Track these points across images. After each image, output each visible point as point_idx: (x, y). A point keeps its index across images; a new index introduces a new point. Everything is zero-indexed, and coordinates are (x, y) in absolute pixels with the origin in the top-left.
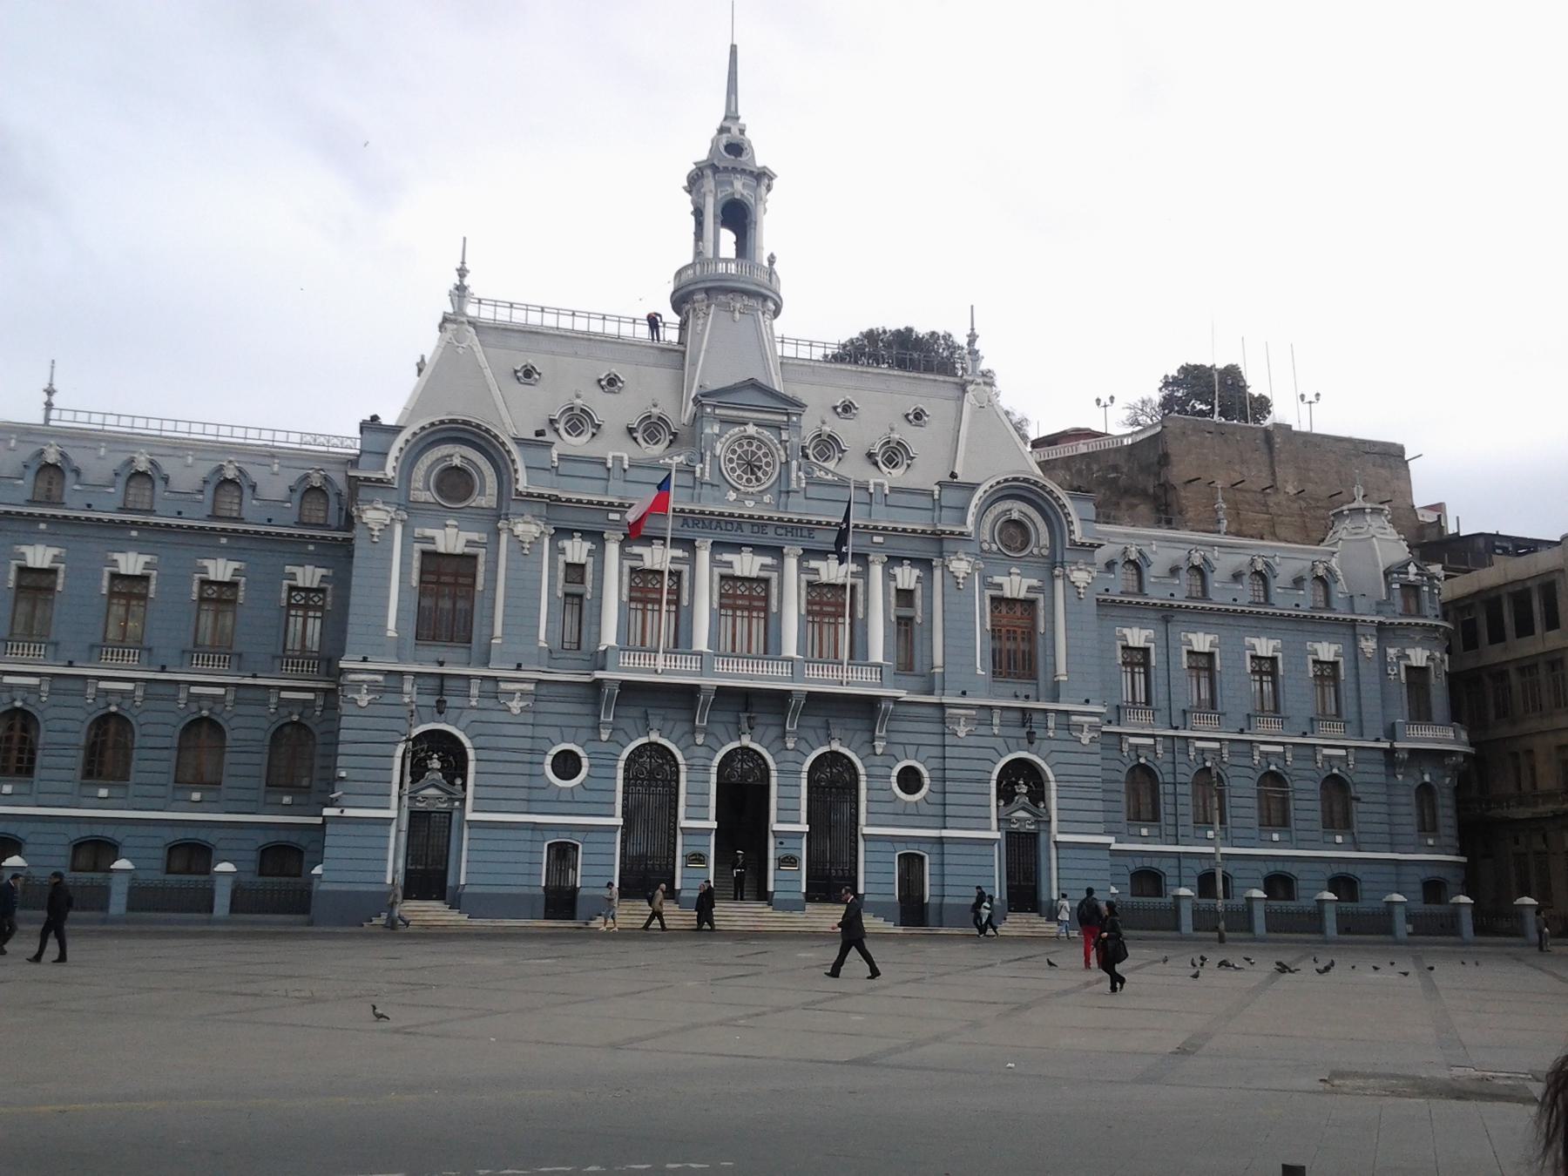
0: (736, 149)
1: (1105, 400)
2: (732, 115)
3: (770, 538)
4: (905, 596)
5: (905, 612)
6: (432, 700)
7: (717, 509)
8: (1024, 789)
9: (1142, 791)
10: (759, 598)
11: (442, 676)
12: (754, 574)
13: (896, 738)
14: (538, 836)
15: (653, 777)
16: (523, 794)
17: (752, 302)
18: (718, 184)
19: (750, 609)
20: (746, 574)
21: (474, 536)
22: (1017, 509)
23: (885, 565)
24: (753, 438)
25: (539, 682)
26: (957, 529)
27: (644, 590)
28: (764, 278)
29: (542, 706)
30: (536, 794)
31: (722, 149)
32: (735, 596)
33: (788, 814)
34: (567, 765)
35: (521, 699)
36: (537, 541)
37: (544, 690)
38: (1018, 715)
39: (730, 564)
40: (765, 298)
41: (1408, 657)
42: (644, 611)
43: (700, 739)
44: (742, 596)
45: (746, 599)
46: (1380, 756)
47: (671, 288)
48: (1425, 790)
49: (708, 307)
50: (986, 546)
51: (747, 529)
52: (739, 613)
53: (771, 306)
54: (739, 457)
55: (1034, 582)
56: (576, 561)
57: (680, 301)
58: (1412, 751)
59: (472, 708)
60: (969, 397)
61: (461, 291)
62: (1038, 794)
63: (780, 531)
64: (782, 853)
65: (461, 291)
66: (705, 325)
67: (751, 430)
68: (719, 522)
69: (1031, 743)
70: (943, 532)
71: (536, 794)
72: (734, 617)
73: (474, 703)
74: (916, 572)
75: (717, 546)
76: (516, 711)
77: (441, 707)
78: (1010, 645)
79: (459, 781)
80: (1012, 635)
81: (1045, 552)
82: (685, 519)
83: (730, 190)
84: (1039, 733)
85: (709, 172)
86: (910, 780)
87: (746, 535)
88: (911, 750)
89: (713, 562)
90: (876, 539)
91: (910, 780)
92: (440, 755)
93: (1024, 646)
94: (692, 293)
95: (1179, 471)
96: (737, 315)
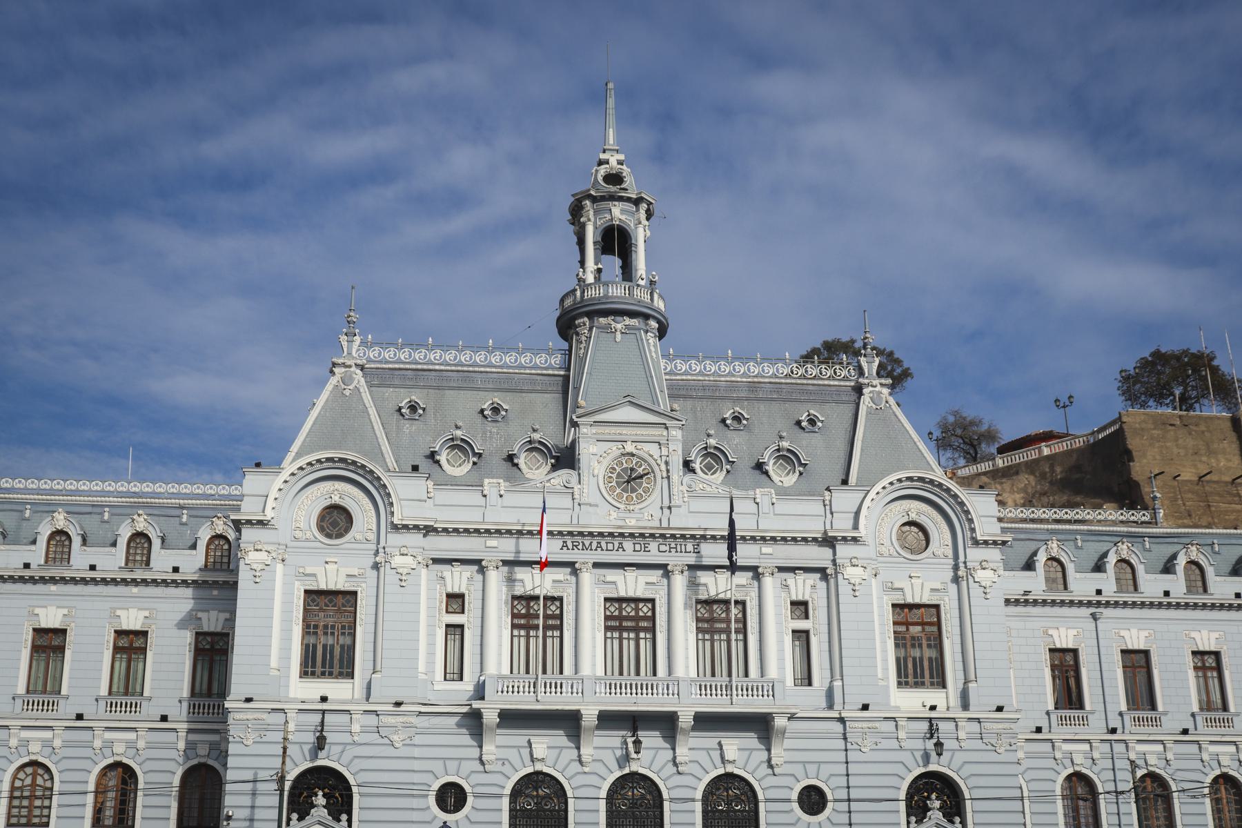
1: (1064, 400)
3: (654, 554)
4: (801, 607)
5: (802, 625)
6: (311, 738)
8: (937, 804)
10: (645, 618)
11: (324, 712)
12: (640, 594)
17: (634, 322)
18: (596, 212)
19: (637, 630)
20: (631, 594)
22: (918, 510)
24: (633, 455)
27: (528, 616)
28: (647, 298)
31: (600, 179)
32: (620, 618)
34: (452, 797)
38: (925, 726)
40: (647, 317)
42: (528, 637)
44: (628, 618)
45: (630, 620)
47: (558, 313)
49: (591, 329)
50: (884, 550)
52: (625, 635)
53: (654, 324)
54: (619, 476)
56: (456, 590)
57: (566, 326)
60: (866, 401)
62: (954, 805)
66: (587, 349)
67: (630, 448)
69: (939, 754)
70: (835, 538)
72: (621, 639)
77: (321, 743)
78: (916, 653)
79: (344, 817)
80: (915, 642)
83: (609, 217)
84: (948, 744)
86: (813, 800)
87: (629, 553)
91: (813, 800)
93: (929, 653)
94: (575, 318)
95: (1140, 469)
96: (619, 336)
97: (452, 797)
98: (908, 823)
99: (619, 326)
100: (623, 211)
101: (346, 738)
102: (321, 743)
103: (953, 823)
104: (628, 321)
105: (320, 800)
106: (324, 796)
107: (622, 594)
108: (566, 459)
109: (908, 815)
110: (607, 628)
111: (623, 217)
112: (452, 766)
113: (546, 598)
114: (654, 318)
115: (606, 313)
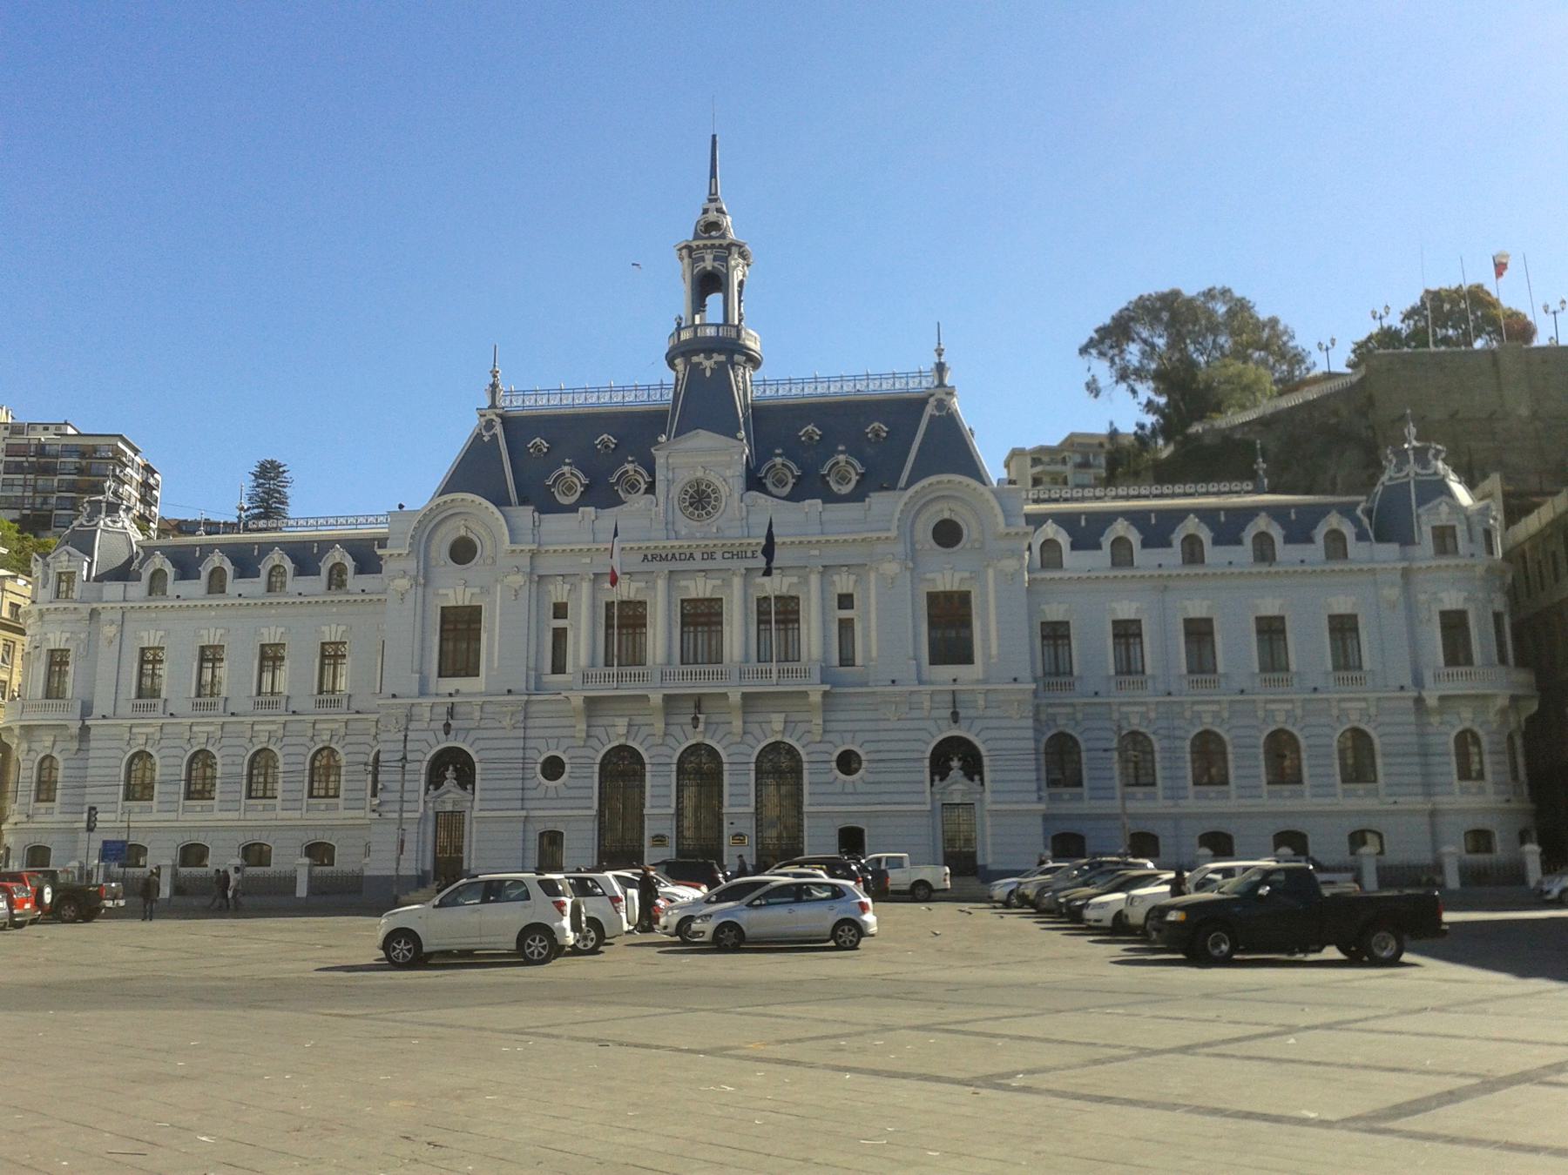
0: (712, 227)
2: (713, 198)
3: (718, 563)
4: (845, 601)
6: (440, 725)
7: (669, 544)
9: (1061, 761)
12: (708, 595)
13: (830, 726)
15: (622, 769)
17: (722, 358)
20: (701, 596)
23: (822, 574)
26: (883, 535)
32: (696, 615)
34: (553, 768)
38: (949, 698)
41: (1441, 600)
44: (702, 615)
45: (701, 618)
46: (1411, 704)
48: (1466, 740)
55: (967, 575)
57: (672, 365)
58: (1442, 698)
60: (930, 410)
61: (494, 386)
62: (973, 766)
64: (734, 832)
65: (494, 386)
67: (700, 474)
74: (853, 578)
81: (977, 545)
84: (962, 713)
85: (685, 252)
88: (849, 736)
91: (848, 762)
92: (452, 766)
96: (708, 374)
97: (553, 768)
98: (932, 781)
100: (715, 259)
101: (467, 724)
102: (447, 728)
103: (972, 780)
105: (450, 774)
106: (456, 770)
107: (694, 596)
108: (651, 489)
109: (932, 774)
110: (683, 624)
112: (552, 743)
113: (622, 603)
115: (697, 353)
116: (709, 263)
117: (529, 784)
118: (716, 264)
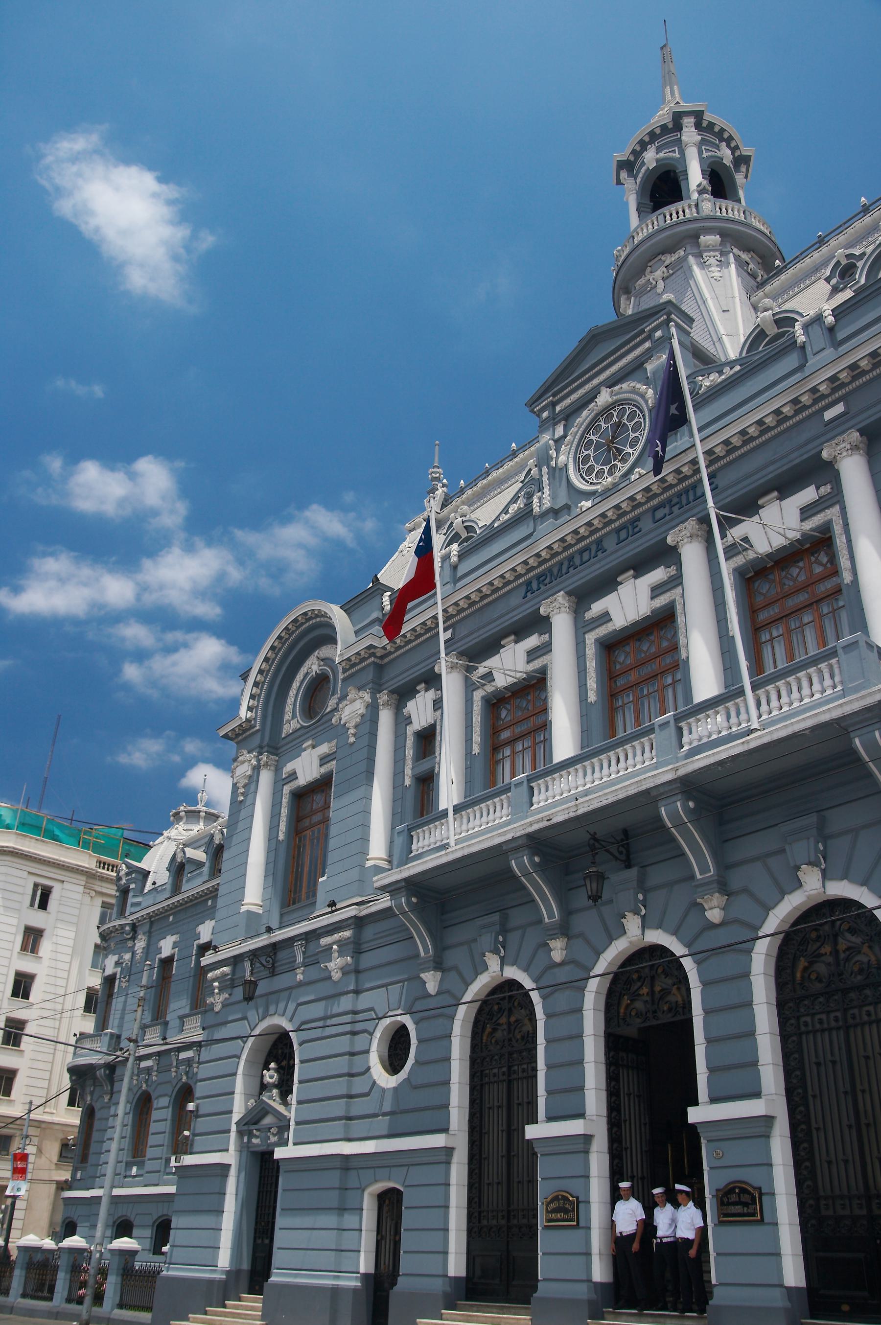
14: (353, 1180)
16: (338, 1108)
21: (324, 749)
25: (359, 922)
29: (367, 960)
30: (359, 1107)
33: (739, 1082)
35: (341, 954)
36: (371, 719)
37: (369, 932)
39: (605, 617)
43: (558, 950)
51: (610, 544)
59: (301, 984)
63: (659, 514)
67: (604, 397)
68: (571, 558)
71: (359, 1107)
73: (300, 977)
75: (581, 599)
76: (336, 976)
82: (529, 583)
89: (581, 627)
90: (828, 415)
99: (658, 274)
104: (669, 259)
111: (661, 155)
114: (709, 231)
116: (651, 157)
117: (359, 1085)
118: (661, 155)
